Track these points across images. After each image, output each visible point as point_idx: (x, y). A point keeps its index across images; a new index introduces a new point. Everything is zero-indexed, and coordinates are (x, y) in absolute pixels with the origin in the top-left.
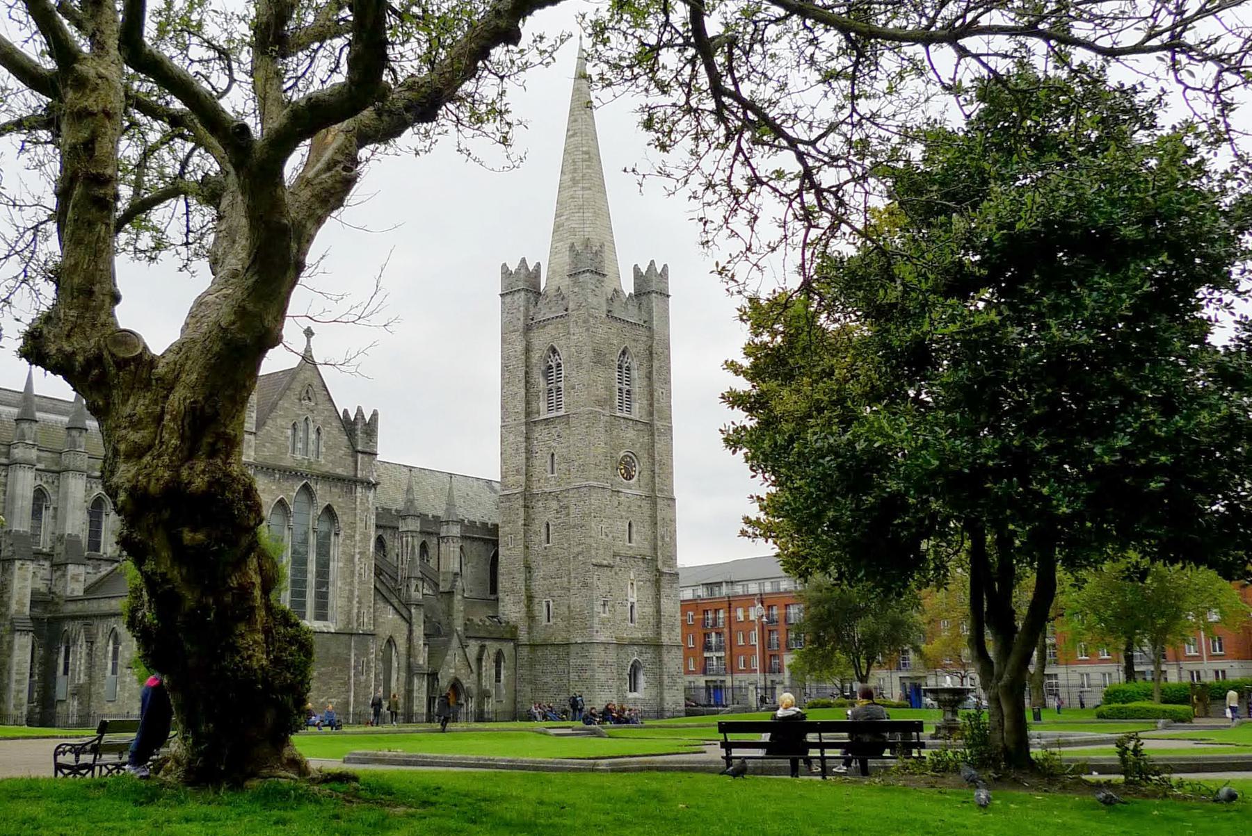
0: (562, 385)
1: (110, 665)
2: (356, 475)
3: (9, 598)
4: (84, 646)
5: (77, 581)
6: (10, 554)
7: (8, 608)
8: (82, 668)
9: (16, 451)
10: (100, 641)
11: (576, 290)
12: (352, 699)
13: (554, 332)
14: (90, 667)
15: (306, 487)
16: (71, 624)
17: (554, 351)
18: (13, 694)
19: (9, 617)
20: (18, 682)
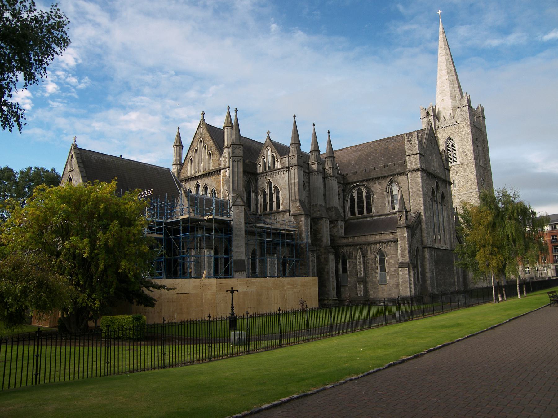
0: (456, 152)
1: (379, 267)
2: (446, 179)
3: (322, 237)
4: (362, 259)
5: (342, 229)
6: (318, 215)
7: (322, 241)
8: (362, 269)
9: (313, 166)
10: (370, 256)
11: (462, 113)
12: (456, 279)
13: (450, 131)
14: (366, 268)
15: (437, 185)
16: (345, 249)
17: (449, 139)
18: (331, 283)
19: (323, 246)
20: (332, 277)
